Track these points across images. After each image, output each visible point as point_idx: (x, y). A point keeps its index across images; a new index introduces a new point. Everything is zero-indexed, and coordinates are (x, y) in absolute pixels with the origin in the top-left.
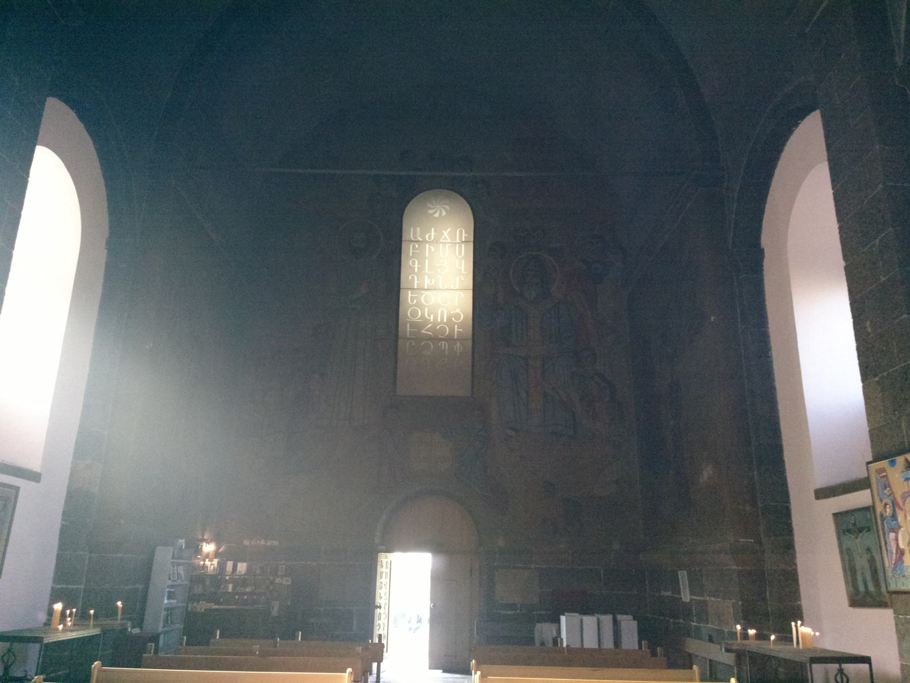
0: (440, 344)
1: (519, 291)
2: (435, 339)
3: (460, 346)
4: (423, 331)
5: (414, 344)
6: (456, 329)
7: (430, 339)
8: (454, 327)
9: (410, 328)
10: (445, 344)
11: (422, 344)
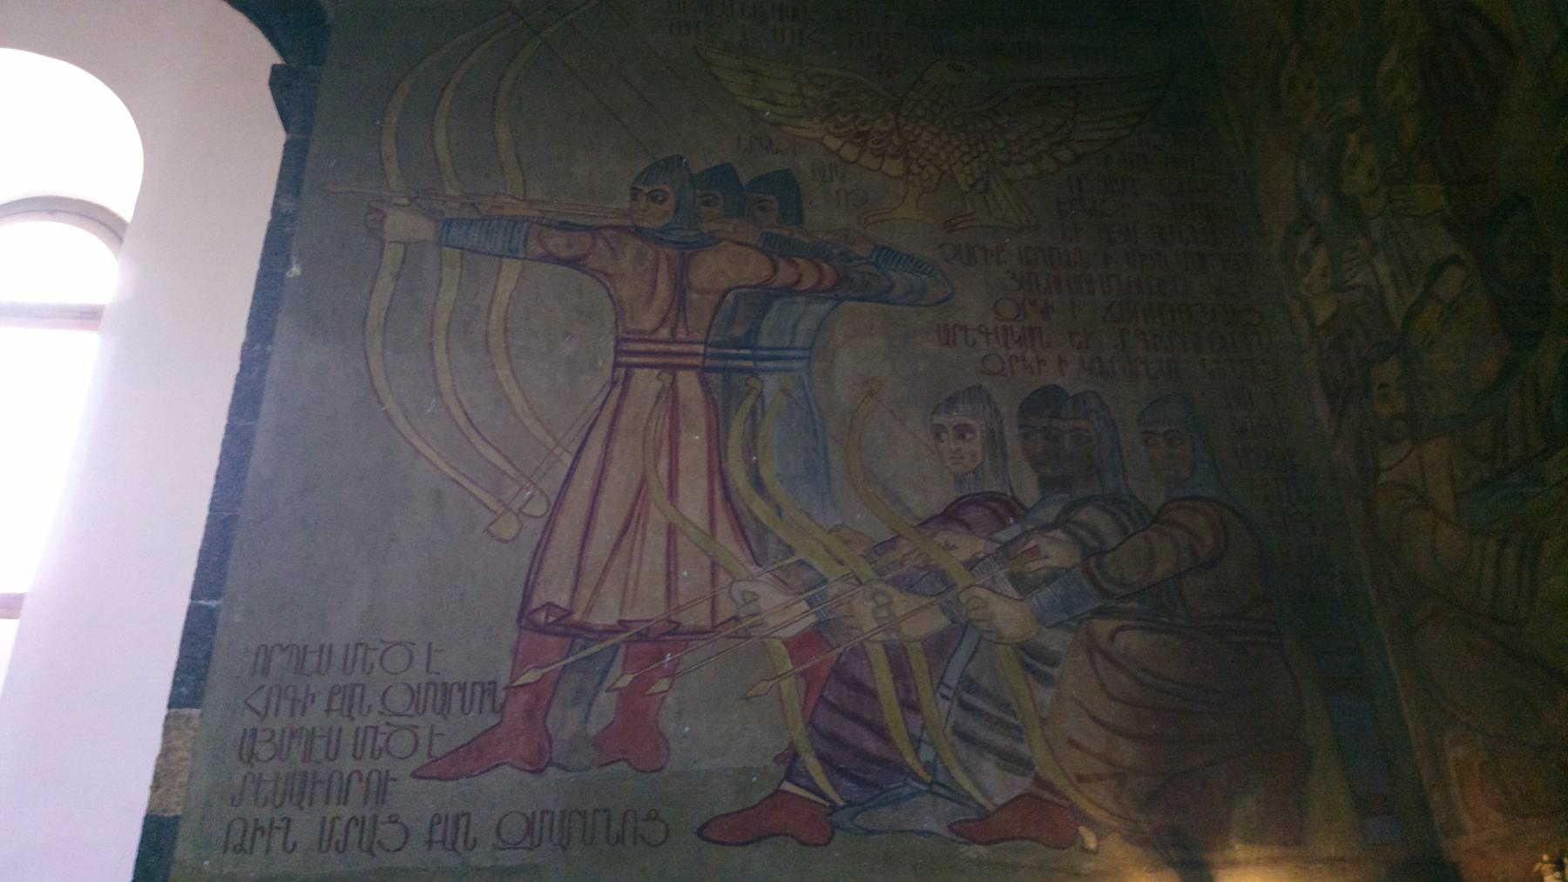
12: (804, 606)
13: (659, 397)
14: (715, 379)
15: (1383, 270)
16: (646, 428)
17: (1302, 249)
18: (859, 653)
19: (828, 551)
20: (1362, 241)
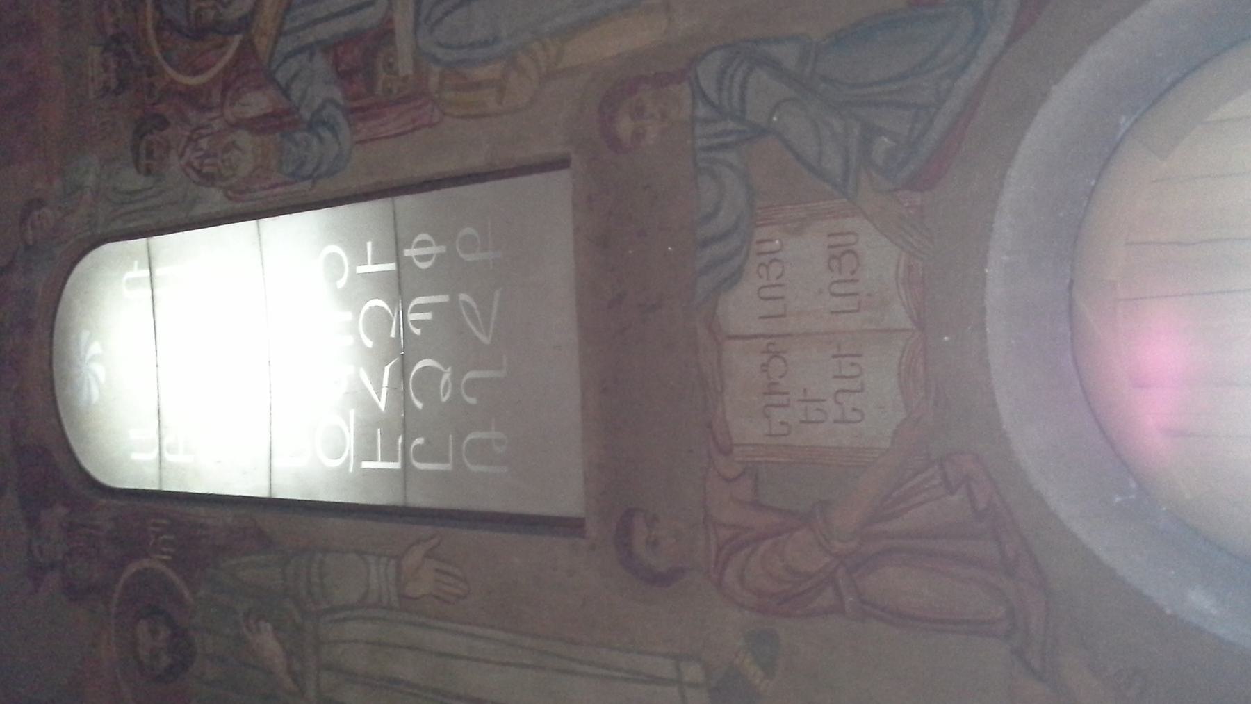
0: (417, 332)
1: (237, 40)
4: (382, 405)
5: (419, 441)
7: (403, 370)
8: (365, 275)
9: (374, 459)
10: (418, 309)
11: (419, 405)
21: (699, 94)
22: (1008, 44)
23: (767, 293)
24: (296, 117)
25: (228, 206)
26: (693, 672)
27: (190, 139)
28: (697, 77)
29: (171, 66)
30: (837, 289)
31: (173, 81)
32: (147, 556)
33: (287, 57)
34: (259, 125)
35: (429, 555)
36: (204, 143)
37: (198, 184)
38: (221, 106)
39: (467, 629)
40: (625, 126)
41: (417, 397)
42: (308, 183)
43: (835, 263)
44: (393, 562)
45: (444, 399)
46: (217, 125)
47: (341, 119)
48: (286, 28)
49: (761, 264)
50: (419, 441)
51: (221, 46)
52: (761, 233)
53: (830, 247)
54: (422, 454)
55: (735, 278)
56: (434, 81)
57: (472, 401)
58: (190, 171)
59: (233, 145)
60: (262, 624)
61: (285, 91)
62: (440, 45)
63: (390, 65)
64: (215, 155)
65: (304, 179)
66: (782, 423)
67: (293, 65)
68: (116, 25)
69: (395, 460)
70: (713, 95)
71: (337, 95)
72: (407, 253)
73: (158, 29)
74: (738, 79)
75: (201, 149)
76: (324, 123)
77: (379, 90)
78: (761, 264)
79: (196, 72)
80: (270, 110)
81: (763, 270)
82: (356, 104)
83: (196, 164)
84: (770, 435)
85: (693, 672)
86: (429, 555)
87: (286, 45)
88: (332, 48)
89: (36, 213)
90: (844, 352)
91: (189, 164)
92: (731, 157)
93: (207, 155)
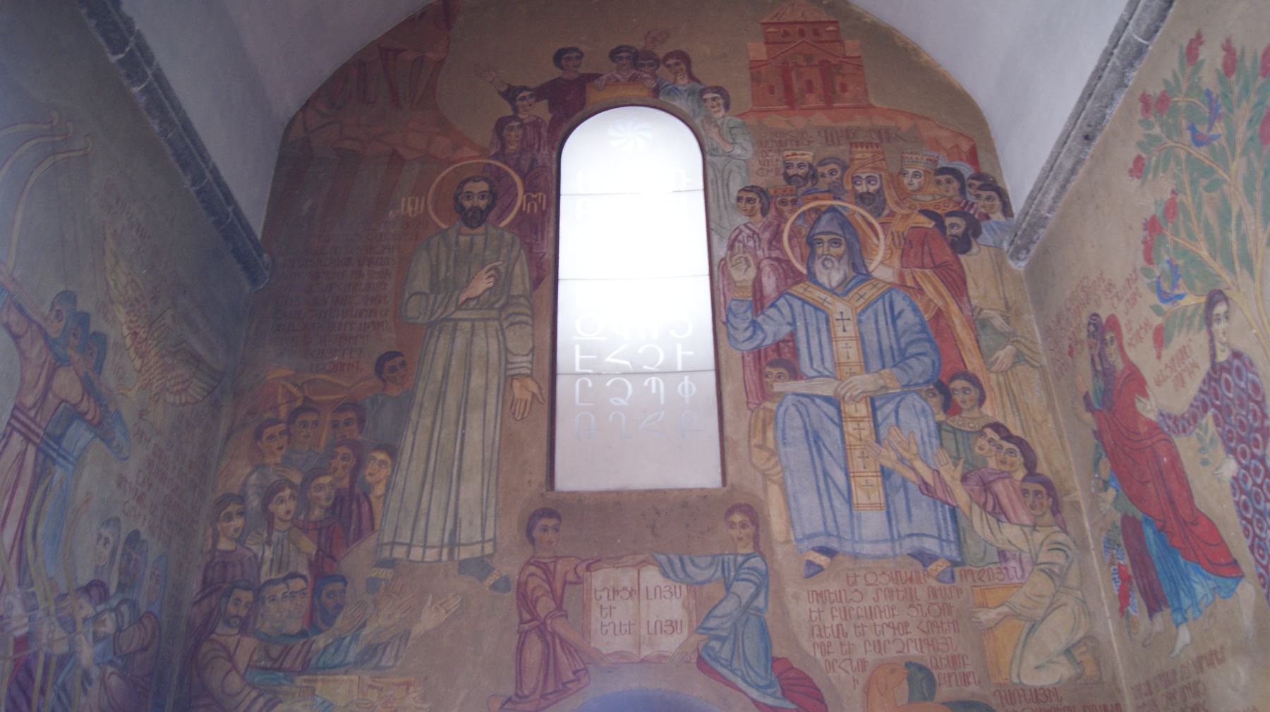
0: (646, 383)
1: (804, 271)
2: (637, 374)
3: (690, 387)
4: (609, 359)
6: (680, 354)
9: (582, 353)
10: (658, 384)
11: (608, 384)
12: (26, 620)
13: (17, 457)
14: (41, 457)
15: (268, 553)
16: (6, 476)
17: (230, 509)
18: (36, 655)
19: (45, 590)
20: (265, 535)
21: (748, 557)
22: (754, 701)
23: (658, 589)
24: (759, 312)
25: (716, 261)
26: (489, 549)
27: (754, 232)
28: (754, 557)
29: (796, 219)
30: (658, 625)
31: (787, 220)
32: (525, 192)
33: (791, 306)
34: (758, 283)
35: (534, 395)
36: (751, 244)
37: (729, 239)
38: (770, 258)
39: (499, 418)
40: (737, 518)
41: (613, 382)
42: (724, 320)
43: (669, 623)
44: (529, 372)
45: (611, 400)
46: (760, 253)
47: (756, 343)
48: (807, 307)
49: (670, 588)
50: (590, 384)
51: (802, 260)
52: (684, 588)
53: (676, 622)
54: (584, 384)
55: (665, 574)
56: (768, 405)
57: (611, 418)
58: (737, 231)
59: (749, 266)
60: (492, 279)
61: (773, 305)
62: (786, 409)
63: (779, 377)
64: (744, 252)
65: (727, 316)
66: (601, 597)
67: (786, 311)
68: (823, 175)
69: (581, 368)
70: (746, 565)
71: (768, 342)
72: (686, 378)
73: (816, 210)
74: (752, 578)
75: (748, 241)
76: (754, 332)
77: (768, 369)
78: (670, 588)
79: (790, 239)
80: (765, 293)
81: (668, 588)
82: (762, 354)
83: (740, 237)
84: (595, 591)
85: (489, 549)
86: (534, 395)
87: (797, 304)
88: (793, 335)
89: (721, 101)
90: (632, 627)
91: (741, 232)
92: (719, 573)
93: (745, 246)
